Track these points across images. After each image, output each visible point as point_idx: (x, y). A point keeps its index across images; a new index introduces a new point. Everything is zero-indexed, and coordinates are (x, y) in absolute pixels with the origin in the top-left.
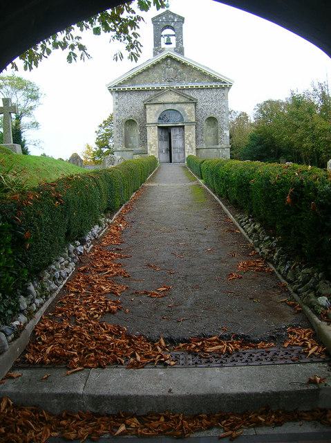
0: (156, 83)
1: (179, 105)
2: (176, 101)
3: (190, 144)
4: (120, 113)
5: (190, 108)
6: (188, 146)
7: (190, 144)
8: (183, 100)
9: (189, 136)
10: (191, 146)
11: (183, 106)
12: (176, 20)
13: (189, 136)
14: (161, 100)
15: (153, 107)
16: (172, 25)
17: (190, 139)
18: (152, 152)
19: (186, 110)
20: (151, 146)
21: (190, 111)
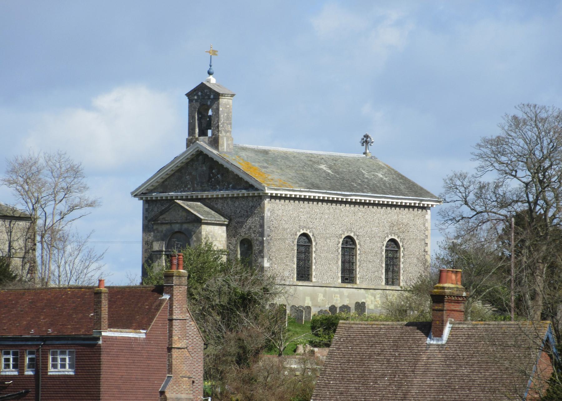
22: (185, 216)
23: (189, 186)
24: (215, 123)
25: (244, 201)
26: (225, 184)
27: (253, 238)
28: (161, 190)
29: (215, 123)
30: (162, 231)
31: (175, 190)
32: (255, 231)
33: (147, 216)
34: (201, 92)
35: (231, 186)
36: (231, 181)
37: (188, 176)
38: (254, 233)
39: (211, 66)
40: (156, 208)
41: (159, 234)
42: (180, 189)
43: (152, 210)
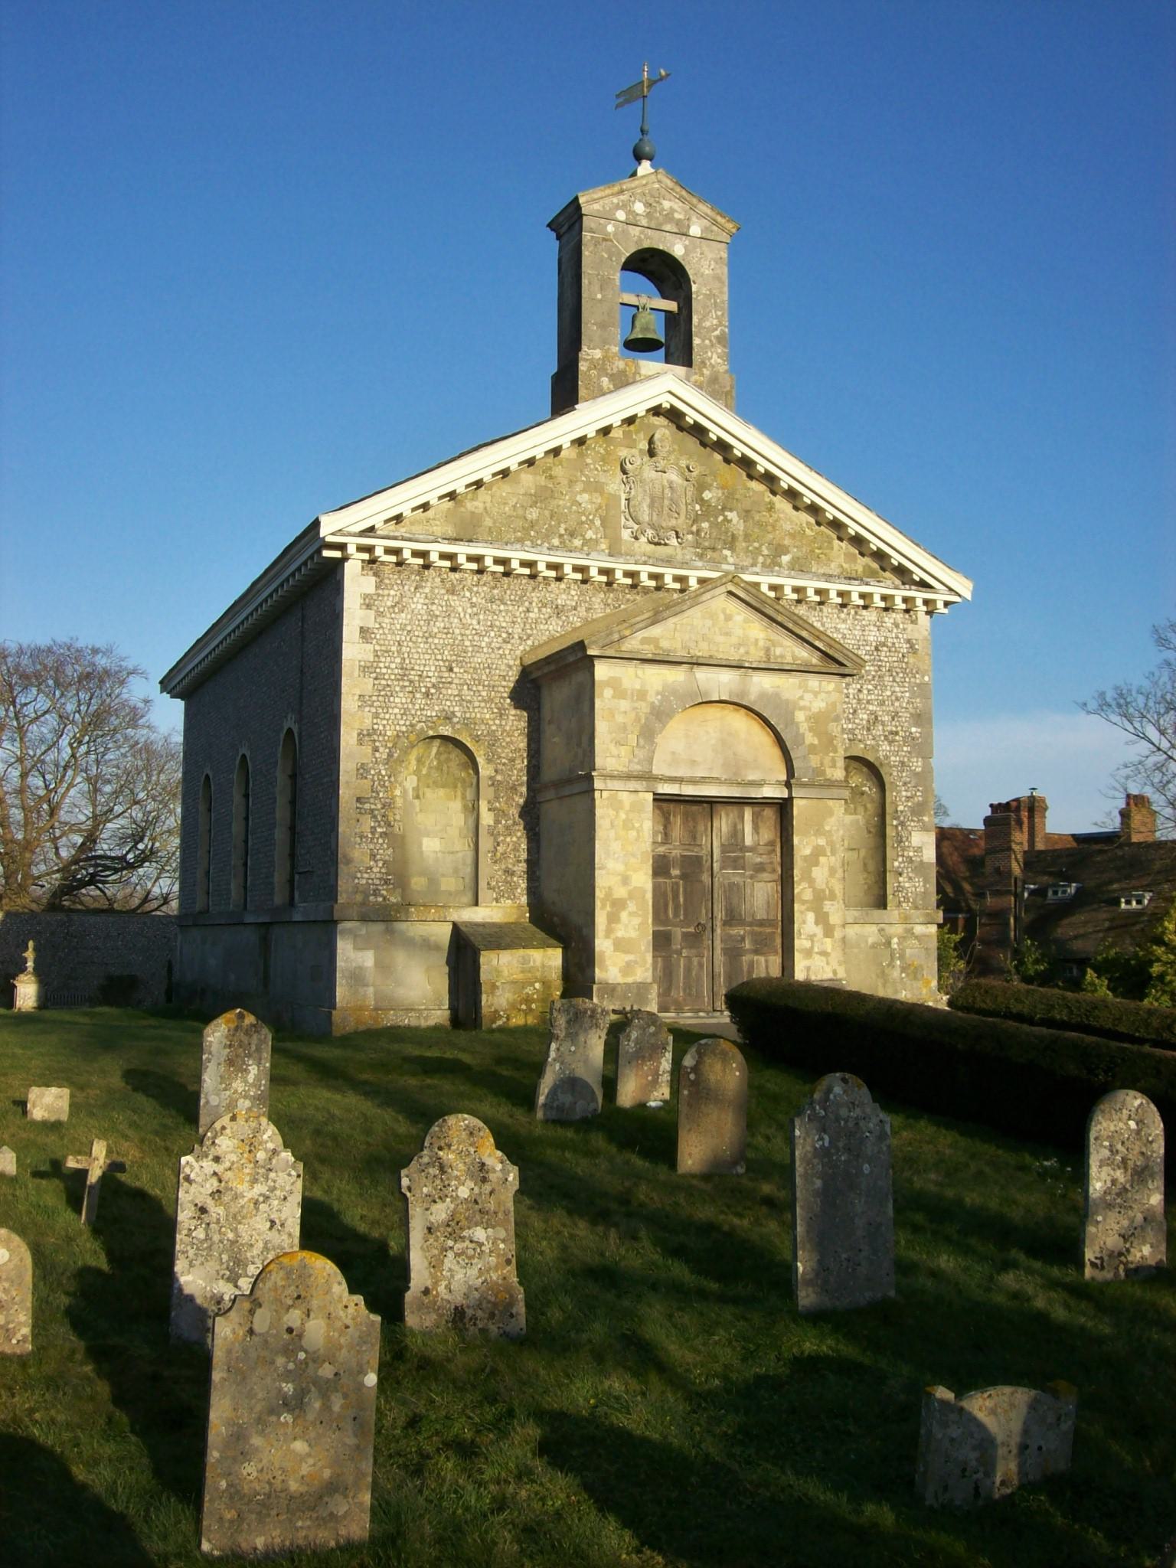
0: (590, 545)
1: (763, 683)
2: (755, 656)
3: (817, 905)
4: (385, 692)
5: (819, 705)
6: (811, 917)
7: (817, 905)
8: (791, 651)
9: (813, 860)
10: (822, 919)
11: (786, 686)
12: (695, 230)
13: (818, 852)
14: (667, 635)
15: (630, 675)
16: (678, 250)
17: (820, 874)
18: (620, 945)
19: (800, 716)
20: (619, 905)
21: (818, 721)
22: (761, 643)
23: (590, 534)
24: (707, 324)
25: (844, 621)
26: (758, 550)
27: (887, 757)
28: (450, 531)
29: (707, 324)
30: (642, 695)
31: (520, 541)
32: (897, 733)
33: (371, 624)
34: (648, 205)
35: (785, 559)
36: (787, 542)
37: (586, 496)
38: (891, 743)
39: (642, 131)
40: (419, 598)
41: (624, 705)
42: (547, 537)
43: (399, 606)
